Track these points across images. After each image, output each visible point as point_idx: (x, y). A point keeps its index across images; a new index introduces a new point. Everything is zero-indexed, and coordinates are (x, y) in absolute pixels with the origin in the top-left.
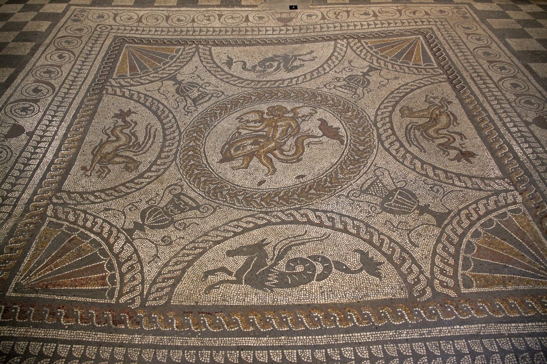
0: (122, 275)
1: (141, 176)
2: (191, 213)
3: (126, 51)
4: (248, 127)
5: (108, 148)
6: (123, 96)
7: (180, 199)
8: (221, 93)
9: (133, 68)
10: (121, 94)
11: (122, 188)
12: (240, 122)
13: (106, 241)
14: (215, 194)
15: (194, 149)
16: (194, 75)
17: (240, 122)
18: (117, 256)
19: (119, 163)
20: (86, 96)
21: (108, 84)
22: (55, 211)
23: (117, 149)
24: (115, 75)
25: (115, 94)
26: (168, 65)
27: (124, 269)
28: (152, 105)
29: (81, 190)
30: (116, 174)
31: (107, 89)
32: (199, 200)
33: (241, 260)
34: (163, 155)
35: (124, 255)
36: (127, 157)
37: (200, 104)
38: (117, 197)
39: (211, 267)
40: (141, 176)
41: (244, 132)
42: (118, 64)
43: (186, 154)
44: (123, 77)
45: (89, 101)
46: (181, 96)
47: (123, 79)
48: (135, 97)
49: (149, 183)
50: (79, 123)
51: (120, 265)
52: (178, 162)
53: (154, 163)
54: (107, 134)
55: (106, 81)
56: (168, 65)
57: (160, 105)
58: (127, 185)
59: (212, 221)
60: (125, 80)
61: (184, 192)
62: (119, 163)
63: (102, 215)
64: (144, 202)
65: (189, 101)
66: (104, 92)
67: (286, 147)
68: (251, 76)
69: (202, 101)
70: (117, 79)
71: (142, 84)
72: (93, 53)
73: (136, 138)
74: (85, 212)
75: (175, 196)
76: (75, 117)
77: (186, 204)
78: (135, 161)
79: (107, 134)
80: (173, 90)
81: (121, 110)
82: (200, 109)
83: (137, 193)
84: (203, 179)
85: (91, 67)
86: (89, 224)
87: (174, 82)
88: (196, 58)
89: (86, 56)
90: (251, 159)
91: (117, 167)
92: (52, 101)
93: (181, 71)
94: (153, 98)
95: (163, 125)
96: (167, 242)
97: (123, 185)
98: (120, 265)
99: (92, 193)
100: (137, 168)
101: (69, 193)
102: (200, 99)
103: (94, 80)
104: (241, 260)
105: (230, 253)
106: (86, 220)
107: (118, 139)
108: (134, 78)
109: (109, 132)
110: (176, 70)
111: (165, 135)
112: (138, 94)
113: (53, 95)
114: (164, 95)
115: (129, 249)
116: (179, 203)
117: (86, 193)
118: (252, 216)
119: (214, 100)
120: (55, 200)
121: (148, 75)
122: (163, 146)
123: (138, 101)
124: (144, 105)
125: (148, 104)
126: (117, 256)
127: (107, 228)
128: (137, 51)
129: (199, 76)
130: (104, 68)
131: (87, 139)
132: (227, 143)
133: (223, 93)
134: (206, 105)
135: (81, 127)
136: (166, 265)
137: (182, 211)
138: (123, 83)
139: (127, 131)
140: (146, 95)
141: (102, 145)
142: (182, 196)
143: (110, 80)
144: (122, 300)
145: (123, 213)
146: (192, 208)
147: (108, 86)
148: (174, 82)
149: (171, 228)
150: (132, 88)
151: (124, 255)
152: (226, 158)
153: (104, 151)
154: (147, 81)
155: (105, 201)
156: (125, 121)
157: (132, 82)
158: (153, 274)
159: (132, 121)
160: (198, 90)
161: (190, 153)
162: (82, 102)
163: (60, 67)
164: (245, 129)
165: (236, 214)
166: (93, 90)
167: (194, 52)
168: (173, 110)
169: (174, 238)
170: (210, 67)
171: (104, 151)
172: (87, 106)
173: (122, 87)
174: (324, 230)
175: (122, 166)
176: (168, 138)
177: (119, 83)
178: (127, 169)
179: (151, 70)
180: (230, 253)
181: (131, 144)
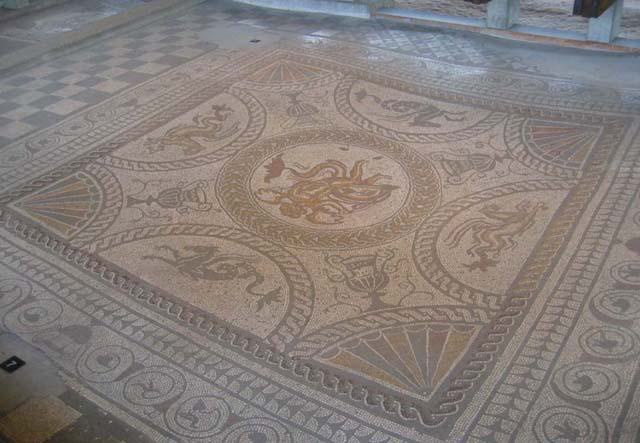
0: (520, 131)
1: (483, 200)
2: (451, 157)
3: (436, 382)
4: (339, 210)
5: (513, 228)
6: (473, 291)
7: (455, 172)
8: (330, 260)
9: (438, 340)
10: (476, 294)
11: (505, 191)
12: (342, 218)
13: (528, 153)
14: (423, 163)
15: (414, 209)
16: (341, 300)
17: (342, 218)
18: (522, 142)
19: (503, 213)
20: (536, 293)
21: (495, 314)
22: (574, 174)
23: (502, 227)
24: (477, 331)
25: (486, 295)
26: (371, 332)
27: (518, 134)
28: (436, 271)
29: (550, 192)
30: (510, 204)
31: (497, 304)
32: (438, 165)
33: (434, 121)
34: (451, 214)
35: (517, 142)
36: (494, 217)
37: (369, 255)
38: (514, 184)
39: (456, 123)
40: (483, 200)
41: (349, 207)
42: (463, 354)
43: (431, 197)
44: (464, 327)
45: (532, 285)
46: (385, 274)
47: (464, 321)
48: (455, 287)
49: (478, 193)
50: (549, 254)
51: (520, 137)
52: (438, 205)
53: (463, 209)
54: (512, 242)
55: (495, 321)
56: (371, 332)
57: (424, 269)
58: (500, 194)
59: (437, 148)
60: (460, 319)
61: (447, 175)
62: (503, 213)
63: (530, 171)
64: (488, 177)
65: (379, 265)
66: (503, 298)
67: (330, 175)
68: (267, 267)
69: (361, 259)
70: (476, 323)
71: (434, 308)
72: (511, 390)
73: (474, 236)
74: (546, 174)
75: (457, 175)
76: (555, 262)
77: (451, 166)
78: (484, 213)
79: (512, 242)
80: (391, 287)
81: (484, 270)
82: (372, 251)
83: (491, 185)
84: (424, 179)
85: (519, 352)
86: (543, 165)
87: (381, 298)
88: (311, 327)
89: (528, 381)
90: (366, 181)
91: (508, 210)
92: (593, 285)
93: (355, 315)
94: (428, 280)
95: (434, 244)
96: (479, 144)
97: (504, 194)
98: (520, 137)
99: (537, 189)
100: (486, 207)
101: (562, 188)
102: (363, 262)
103: (518, 324)
104: (434, 121)
105: (438, 126)
106: (546, 168)
107: (498, 237)
108: (444, 321)
109: (510, 244)
110: (363, 318)
111: (438, 233)
112: (448, 291)
113: (592, 295)
114: (410, 282)
115: (512, 145)
116: (457, 168)
117: (544, 189)
118: (405, 141)
119: (345, 255)
120: (576, 182)
121: (417, 321)
122: (447, 222)
123: (453, 280)
124: (446, 274)
125: (440, 274)
126: (522, 142)
127: (527, 162)
128: (410, 376)
129: (336, 296)
130: (494, 348)
131: (539, 236)
132: (375, 202)
133: (326, 259)
134: (360, 252)
135: (546, 249)
136: (486, 130)
137: (457, 162)
138: (466, 313)
139: (484, 244)
140: (438, 287)
141: (521, 231)
142: (451, 171)
143: (489, 321)
144: (522, 119)
145: (510, 170)
146: (448, 161)
147: (493, 311)
148: (381, 298)
149: (472, 153)
150: (454, 303)
151: (517, 142)
152: (388, 189)
153: (519, 225)
154: (423, 310)
155: (525, 182)
156: (483, 256)
157: (450, 313)
158: (497, 127)
159: (473, 255)
160: (355, 274)
161: (419, 206)
162: (544, 281)
163: (586, 357)
164: (344, 208)
165: (416, 147)
166: (523, 303)
167: (304, 339)
168: (410, 258)
169: (474, 146)
170: (305, 303)
171: (519, 225)
172: (535, 277)
173: (470, 308)
174: (370, 118)
175: (501, 211)
176: (435, 229)
177: (473, 315)
178: (496, 207)
179: (405, 331)
180: (438, 126)
181: (483, 230)
